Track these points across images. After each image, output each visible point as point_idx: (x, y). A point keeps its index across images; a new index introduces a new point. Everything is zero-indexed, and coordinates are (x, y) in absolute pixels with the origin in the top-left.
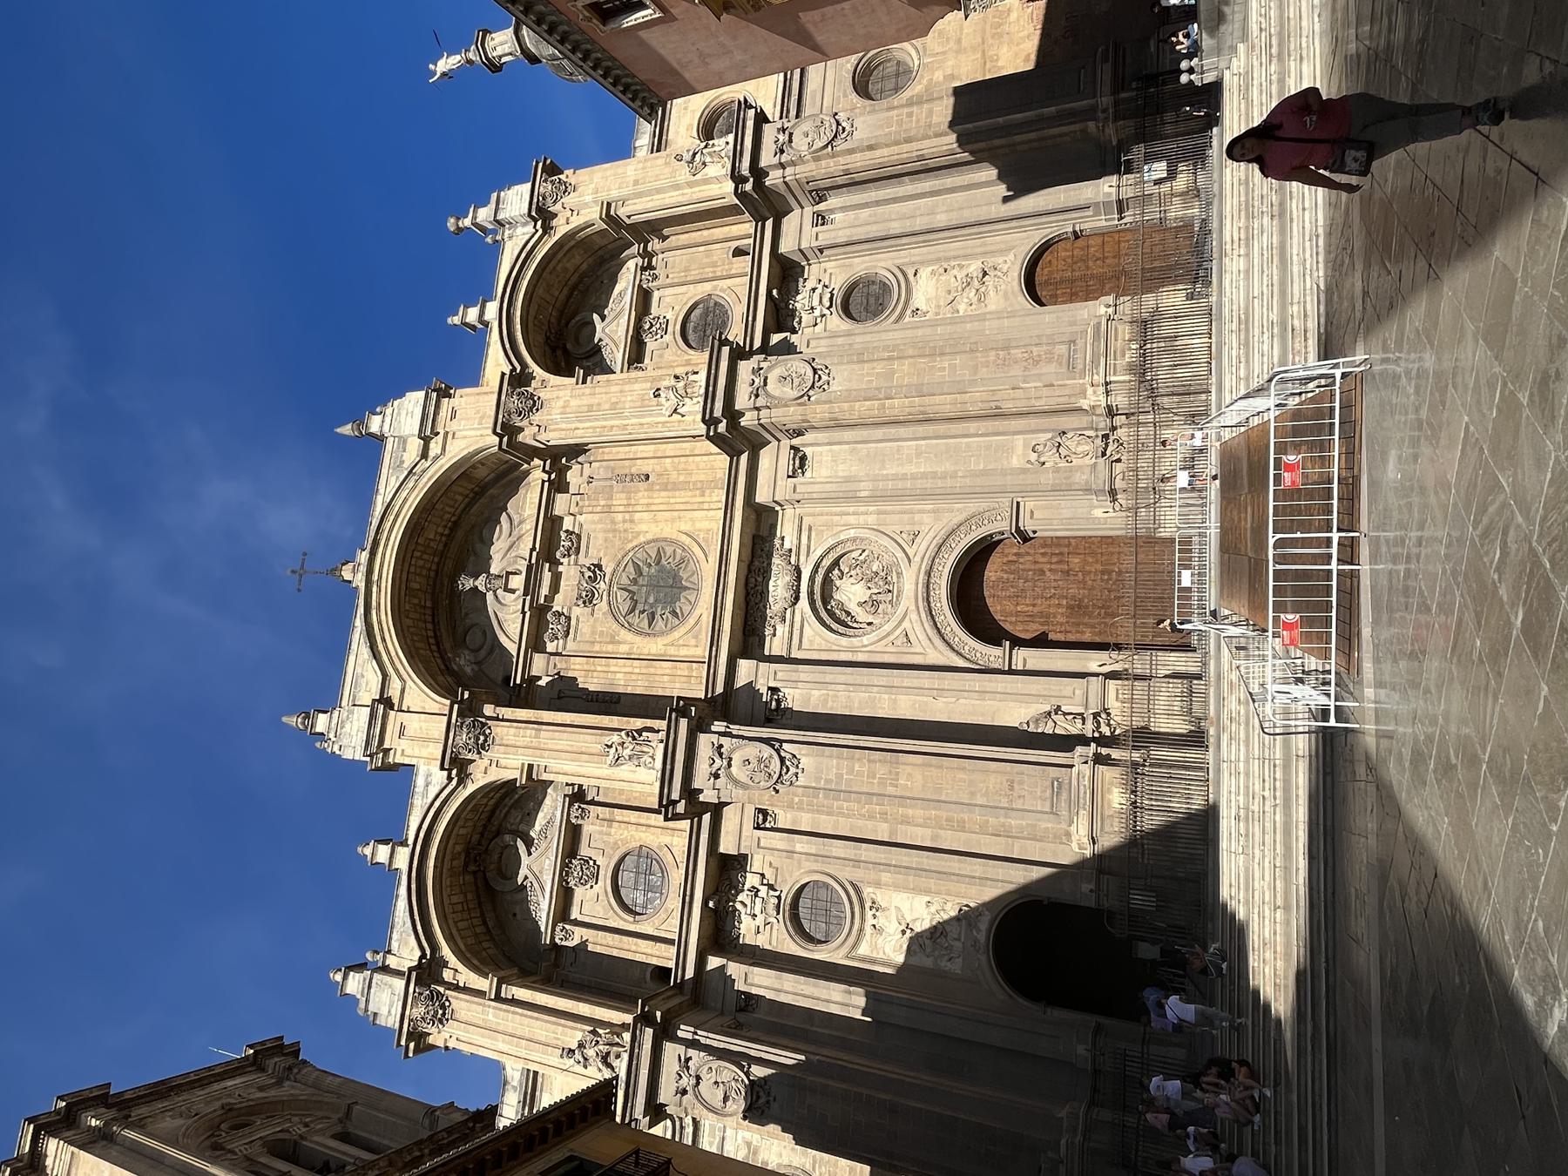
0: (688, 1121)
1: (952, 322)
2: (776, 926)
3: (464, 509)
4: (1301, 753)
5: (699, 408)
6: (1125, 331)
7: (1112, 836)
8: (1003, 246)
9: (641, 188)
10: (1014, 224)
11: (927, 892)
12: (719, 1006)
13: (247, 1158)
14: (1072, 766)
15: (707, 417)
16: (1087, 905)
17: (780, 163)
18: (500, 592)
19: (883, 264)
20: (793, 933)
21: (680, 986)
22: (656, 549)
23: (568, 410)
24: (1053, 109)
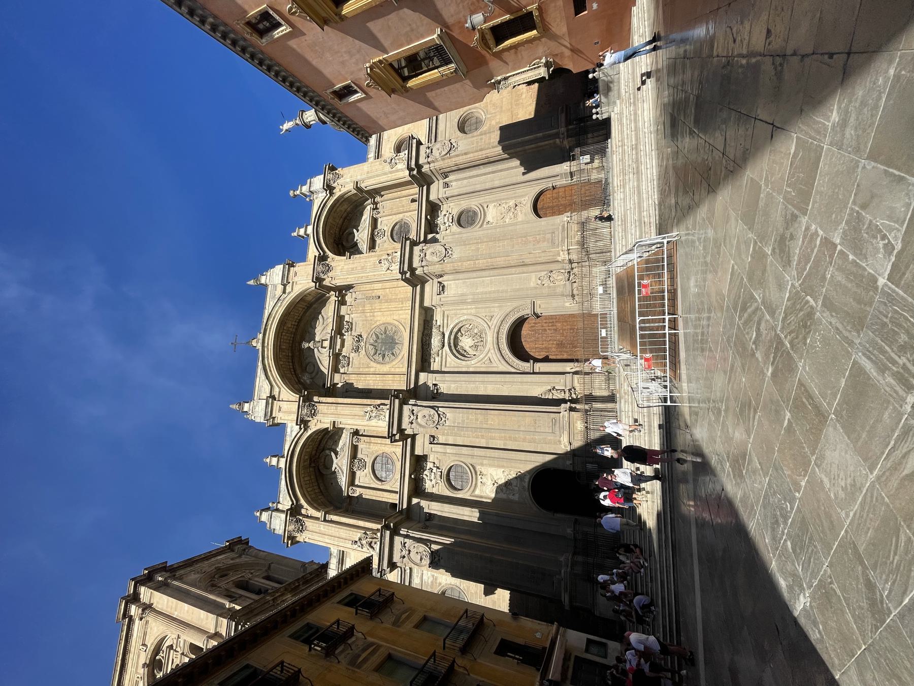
0: (407, 568)
1: (504, 226)
4: (655, 412)
5: (398, 267)
6: (575, 227)
7: (578, 443)
8: (523, 194)
9: (370, 175)
10: (527, 184)
11: (503, 467)
13: (226, 590)
14: (560, 413)
17: (430, 164)
18: (320, 348)
19: (474, 203)
20: (448, 487)
21: (401, 512)
24: (541, 134)
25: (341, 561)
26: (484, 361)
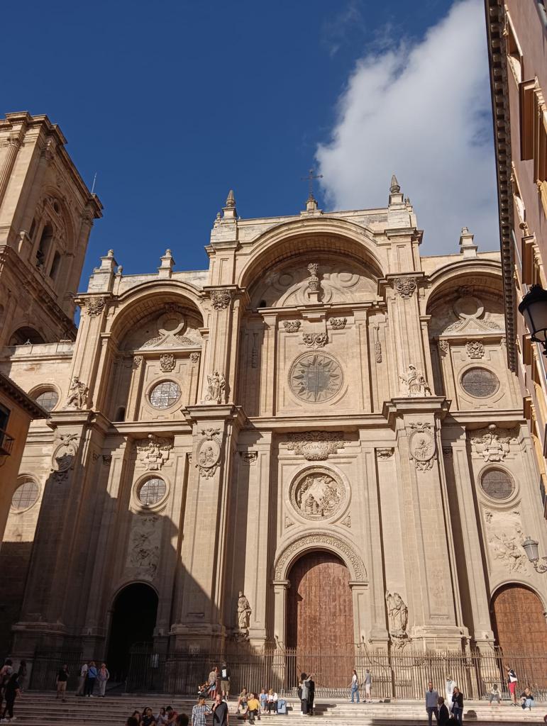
2: (143, 469)
3: (356, 258)
12: (105, 447)
13: (41, 218)
14: (212, 623)
15: (395, 401)
16: (155, 632)
20: (143, 477)
21: (112, 426)
23: (404, 315)
25: (66, 358)
26: (290, 516)
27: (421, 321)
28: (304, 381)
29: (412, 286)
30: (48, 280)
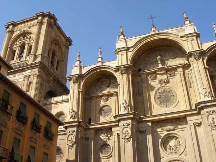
13: (51, 49)
22: (174, 94)
25: (66, 101)
27: (205, 69)
28: (161, 99)
29: (199, 55)
30: (56, 71)
